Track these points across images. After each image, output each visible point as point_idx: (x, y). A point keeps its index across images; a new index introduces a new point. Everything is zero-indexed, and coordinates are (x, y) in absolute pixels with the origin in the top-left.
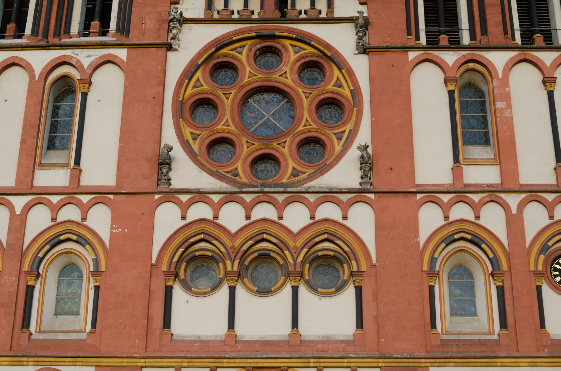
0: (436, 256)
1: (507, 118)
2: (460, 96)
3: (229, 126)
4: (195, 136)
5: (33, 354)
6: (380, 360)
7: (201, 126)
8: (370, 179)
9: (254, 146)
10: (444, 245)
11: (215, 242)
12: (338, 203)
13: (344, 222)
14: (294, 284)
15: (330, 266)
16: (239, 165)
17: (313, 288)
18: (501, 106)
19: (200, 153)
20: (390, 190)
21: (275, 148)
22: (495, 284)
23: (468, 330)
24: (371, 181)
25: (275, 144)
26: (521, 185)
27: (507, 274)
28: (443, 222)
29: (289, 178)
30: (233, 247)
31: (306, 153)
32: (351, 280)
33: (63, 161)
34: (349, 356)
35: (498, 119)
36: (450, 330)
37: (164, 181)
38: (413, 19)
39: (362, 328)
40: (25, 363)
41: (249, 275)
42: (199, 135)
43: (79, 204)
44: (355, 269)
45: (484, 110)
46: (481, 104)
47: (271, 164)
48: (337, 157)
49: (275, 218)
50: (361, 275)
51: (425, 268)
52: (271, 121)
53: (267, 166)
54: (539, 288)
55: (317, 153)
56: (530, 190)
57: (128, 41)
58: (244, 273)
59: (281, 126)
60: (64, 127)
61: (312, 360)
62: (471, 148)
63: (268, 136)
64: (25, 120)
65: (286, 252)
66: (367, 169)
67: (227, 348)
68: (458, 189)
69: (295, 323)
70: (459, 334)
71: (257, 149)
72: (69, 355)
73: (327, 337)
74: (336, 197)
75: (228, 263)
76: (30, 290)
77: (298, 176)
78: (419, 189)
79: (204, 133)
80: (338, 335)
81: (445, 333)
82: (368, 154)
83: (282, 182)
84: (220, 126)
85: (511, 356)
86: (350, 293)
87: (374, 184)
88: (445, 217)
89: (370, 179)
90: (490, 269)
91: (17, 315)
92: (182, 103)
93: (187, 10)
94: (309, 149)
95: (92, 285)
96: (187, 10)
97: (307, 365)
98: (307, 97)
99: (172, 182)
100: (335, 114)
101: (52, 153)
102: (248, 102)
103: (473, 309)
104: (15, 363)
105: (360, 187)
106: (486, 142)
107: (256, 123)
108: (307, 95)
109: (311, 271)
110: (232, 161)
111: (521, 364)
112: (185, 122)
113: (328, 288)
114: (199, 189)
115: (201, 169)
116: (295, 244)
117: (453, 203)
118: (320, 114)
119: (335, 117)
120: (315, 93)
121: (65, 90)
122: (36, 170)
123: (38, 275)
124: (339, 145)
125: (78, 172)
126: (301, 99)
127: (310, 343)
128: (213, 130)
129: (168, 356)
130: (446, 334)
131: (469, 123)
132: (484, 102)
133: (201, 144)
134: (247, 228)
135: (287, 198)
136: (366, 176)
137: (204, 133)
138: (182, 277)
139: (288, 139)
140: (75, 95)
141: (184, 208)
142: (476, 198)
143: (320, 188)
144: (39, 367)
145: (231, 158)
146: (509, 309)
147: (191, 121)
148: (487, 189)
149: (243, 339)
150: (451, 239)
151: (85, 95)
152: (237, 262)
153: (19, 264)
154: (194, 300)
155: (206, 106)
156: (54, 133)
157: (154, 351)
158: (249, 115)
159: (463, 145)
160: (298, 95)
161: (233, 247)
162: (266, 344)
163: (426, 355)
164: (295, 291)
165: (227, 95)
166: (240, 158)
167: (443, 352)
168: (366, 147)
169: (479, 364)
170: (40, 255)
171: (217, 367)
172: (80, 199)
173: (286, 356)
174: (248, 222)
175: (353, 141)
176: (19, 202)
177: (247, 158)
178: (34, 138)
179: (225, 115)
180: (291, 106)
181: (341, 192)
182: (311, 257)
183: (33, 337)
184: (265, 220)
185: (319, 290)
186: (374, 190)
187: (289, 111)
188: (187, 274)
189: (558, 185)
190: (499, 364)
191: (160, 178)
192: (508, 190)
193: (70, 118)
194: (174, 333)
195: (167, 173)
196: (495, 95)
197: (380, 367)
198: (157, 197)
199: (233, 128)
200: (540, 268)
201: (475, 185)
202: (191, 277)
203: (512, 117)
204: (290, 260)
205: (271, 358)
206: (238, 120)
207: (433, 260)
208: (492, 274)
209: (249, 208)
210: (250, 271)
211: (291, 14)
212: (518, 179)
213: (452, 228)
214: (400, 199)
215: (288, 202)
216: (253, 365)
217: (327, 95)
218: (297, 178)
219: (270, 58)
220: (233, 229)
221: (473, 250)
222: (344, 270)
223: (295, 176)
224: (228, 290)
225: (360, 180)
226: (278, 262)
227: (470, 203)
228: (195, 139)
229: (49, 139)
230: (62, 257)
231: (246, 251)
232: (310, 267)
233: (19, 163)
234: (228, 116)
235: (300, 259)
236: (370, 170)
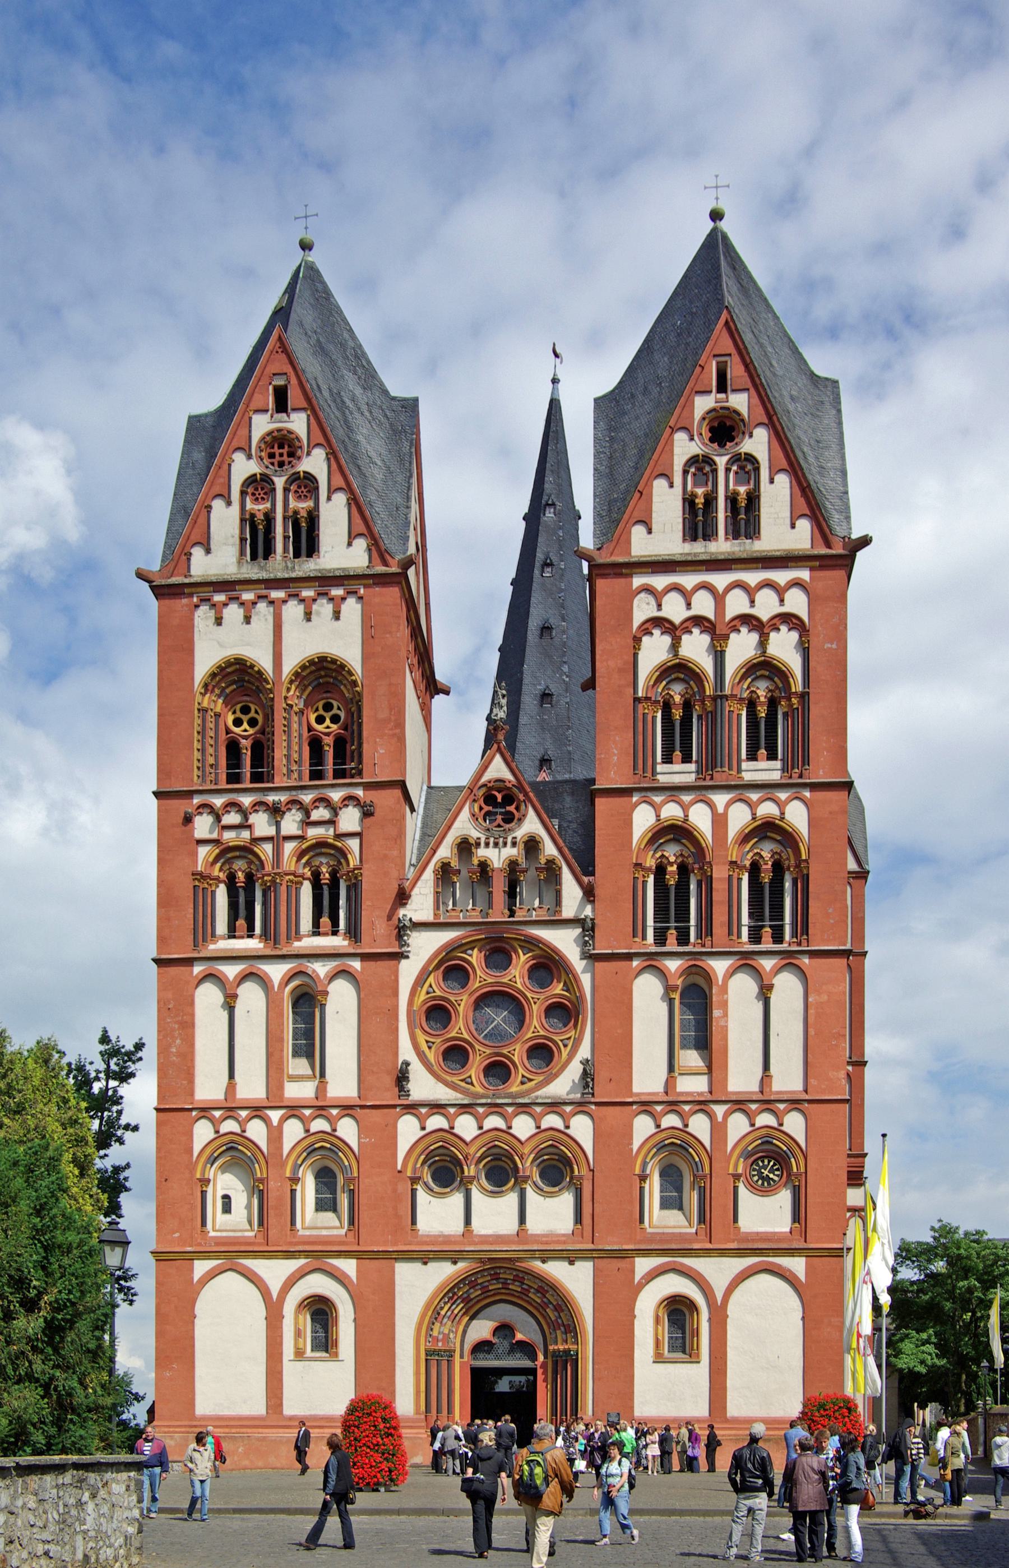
13: (567, 1131)
16: (473, 1073)
23: (672, 1224)
38: (640, 916)
57: (360, 947)
65: (517, 1158)
69: (522, 1219)
93: (416, 910)
96: (416, 910)
99: (411, 1093)
127: (537, 1238)
139: (518, 1047)
151: (323, 1006)
176: (275, 1116)
204: (520, 1165)
211: (520, 916)
213: (663, 1135)
214: (618, 1108)
219: (498, 957)
228: (430, 1048)
235: (528, 1164)
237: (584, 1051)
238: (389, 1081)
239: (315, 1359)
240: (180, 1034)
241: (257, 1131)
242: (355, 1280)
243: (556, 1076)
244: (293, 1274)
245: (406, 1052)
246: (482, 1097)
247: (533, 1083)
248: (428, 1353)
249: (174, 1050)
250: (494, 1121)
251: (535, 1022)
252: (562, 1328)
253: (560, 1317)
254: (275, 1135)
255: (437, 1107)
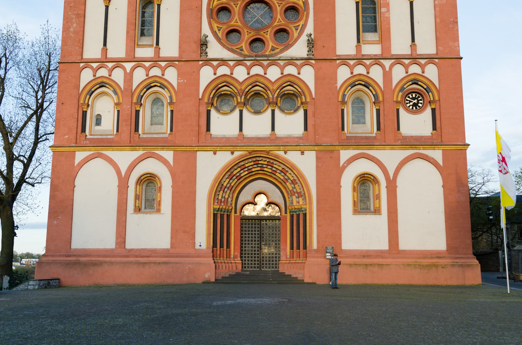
0: (346, 93)
1: (387, 17)
2: (362, 4)
3: (237, 22)
4: (219, 28)
5: (142, 145)
6: (316, 147)
7: (222, 23)
8: (312, 52)
9: (251, 34)
10: (350, 87)
11: (231, 87)
12: (295, 65)
13: (299, 76)
14: (273, 108)
15: (291, 99)
16: (243, 45)
17: (282, 110)
18: (384, 11)
19: (222, 38)
20: (323, 58)
21: (262, 35)
22: (375, 108)
23: (360, 132)
24: (313, 53)
25: (262, 33)
26: (392, 55)
27: (382, 102)
28: (350, 76)
29: (270, 52)
30: (241, 89)
31: (279, 37)
32: (302, 106)
33: (150, 43)
34: (300, 145)
35: (382, 18)
36: (351, 131)
37: (204, 54)
39: (307, 130)
40: (138, 150)
41: (249, 103)
42: (221, 28)
43: (160, 67)
44: (304, 100)
45: (375, 12)
46: (374, 9)
47: (260, 44)
48: (295, 40)
49: (262, 74)
50: (307, 104)
51: (340, 100)
52: (260, 19)
53: (258, 44)
54: (398, 110)
55: (284, 37)
56: (397, 58)
58: (247, 103)
59: (266, 22)
60: (149, 23)
61: (282, 147)
62: (367, 34)
63: (258, 28)
64: (128, 20)
65: (268, 92)
66: (311, 47)
67: (239, 141)
68: (358, 58)
69: (273, 129)
70: (356, 134)
71: (253, 35)
72: (160, 145)
73: (290, 135)
74: (294, 62)
75: (239, 98)
76: (137, 112)
77: (275, 50)
78: (338, 58)
79: (224, 27)
80: (295, 134)
81: (349, 133)
82: (311, 38)
83: (266, 54)
84: (233, 23)
85: (381, 144)
86: (301, 112)
87: (315, 55)
88: (351, 73)
89: (312, 52)
90: (373, 100)
91: (132, 125)
92: (212, 10)
94: (280, 35)
95: (169, 110)
97: (279, 149)
98: (279, 6)
99: (208, 54)
100: (294, 15)
101: (143, 38)
102: (247, 8)
103: (364, 120)
104: (133, 150)
105: (307, 57)
106: (375, 31)
107: (252, 21)
108: (279, 4)
109: (281, 101)
110: (239, 42)
111: (386, 149)
112: (214, 21)
113: (290, 110)
114: (223, 58)
115: (223, 47)
116: (273, 87)
117: (355, 65)
118: (286, 15)
119: (294, 17)
120: (284, 3)
121: (148, 2)
122: (136, 48)
123: (141, 105)
124: (296, 32)
125: (158, 49)
126: (276, 7)
128: (229, 25)
129: (210, 145)
130: (349, 133)
131: (366, 20)
132: (375, 7)
133: (223, 33)
134: (248, 79)
135: (269, 63)
136: (311, 50)
137: (225, 26)
138: (215, 105)
139: (269, 30)
140: (154, 5)
141: (215, 68)
142: (368, 62)
143: (286, 57)
144: (145, 152)
145: (239, 40)
146: (381, 121)
147: (217, 20)
148: (374, 57)
149: (247, 137)
150: (354, 84)
151: (159, 6)
152: (243, 97)
153: (131, 99)
154: (222, 117)
155: (225, 11)
156: (144, 27)
157: (203, 143)
158: (248, 16)
159: (363, 32)
160: (274, 4)
161: (241, 89)
162: (259, 139)
163: (339, 144)
164: (273, 112)
165: (236, 5)
166: (243, 41)
167: (347, 143)
168: (311, 35)
169: (365, 149)
170: (142, 94)
171: (234, 151)
172: (160, 64)
173: (269, 145)
174: (249, 76)
175: (304, 31)
176: (128, 66)
177: (247, 40)
178: (134, 30)
179: (235, 16)
180: (271, 11)
181: (297, 60)
182: (281, 94)
183: (140, 136)
184: (257, 75)
185: (285, 111)
186: (315, 58)
187: (270, 13)
188: (218, 103)
189: (411, 55)
190: (375, 149)
191: (202, 52)
192: (385, 58)
193: (151, 18)
194: (212, 134)
195: (206, 49)
196: (381, 4)
197: (315, 150)
198: (201, 63)
199: (239, 24)
200: (399, 99)
201: (368, 55)
202: (220, 105)
203: (389, 17)
204: (271, 96)
205: (261, 146)
206: (242, 19)
207: (344, 96)
208: (374, 103)
209: (249, 69)
210: (250, 102)
212: (391, 52)
213: (355, 79)
214: (328, 63)
215: (269, 65)
216: (252, 150)
217: (290, 5)
218: (274, 52)
220: (241, 80)
221: (365, 90)
222: (298, 101)
223: (273, 51)
224: (239, 112)
225: (307, 53)
226: (264, 97)
227: (364, 65)
228: (219, 30)
229: (141, 30)
230: (153, 95)
231: (248, 91)
232: (281, 99)
233: (126, 44)
234: (237, 17)
235: (276, 95)
236: (313, 47)
237: (310, 29)
238: (195, 47)
239: (146, 213)
240: (76, 21)
241: (118, 76)
242: (172, 164)
243: (292, 45)
244: (135, 160)
245: (206, 30)
246: (249, 56)
247: (278, 50)
248: (214, 209)
249: (72, 30)
250: (257, 70)
251: (279, 17)
252: (296, 195)
253: (295, 188)
254: (129, 77)
255: (223, 62)
